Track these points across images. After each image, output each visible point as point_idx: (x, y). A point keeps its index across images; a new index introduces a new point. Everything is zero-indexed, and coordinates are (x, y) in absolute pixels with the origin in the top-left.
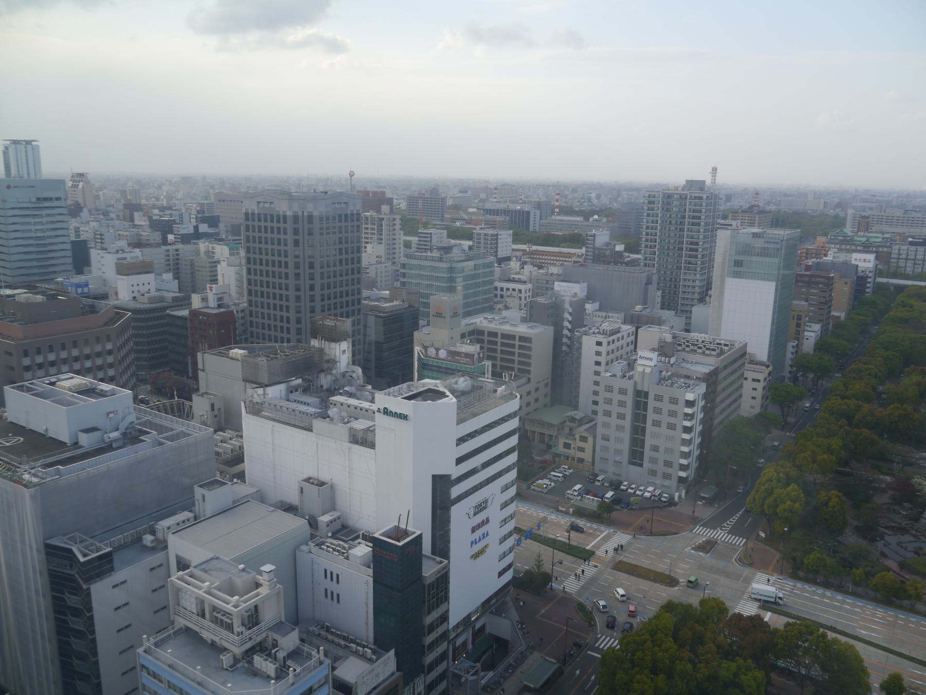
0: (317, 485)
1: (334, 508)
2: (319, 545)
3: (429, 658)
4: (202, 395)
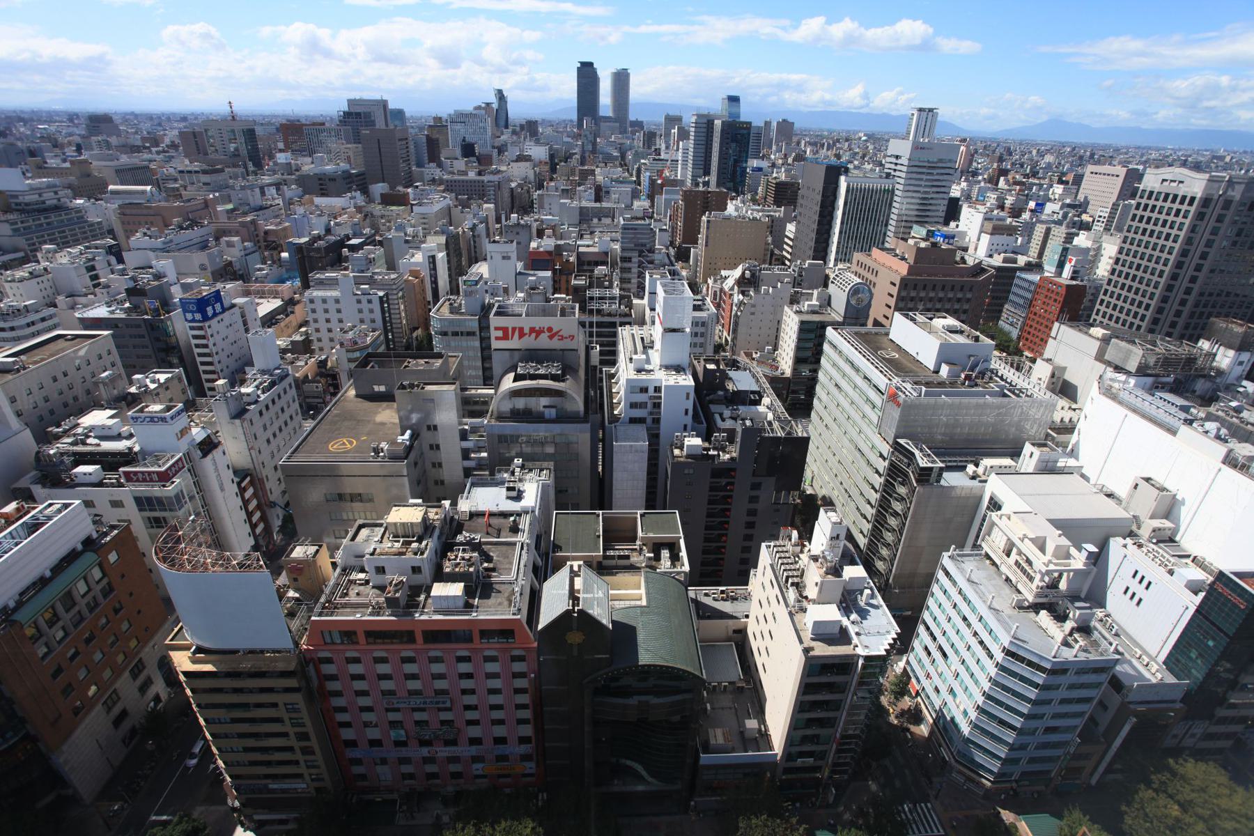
0: (1158, 488)
1: (1167, 516)
2: (1140, 546)
3: (1221, 712)
4: (1048, 360)
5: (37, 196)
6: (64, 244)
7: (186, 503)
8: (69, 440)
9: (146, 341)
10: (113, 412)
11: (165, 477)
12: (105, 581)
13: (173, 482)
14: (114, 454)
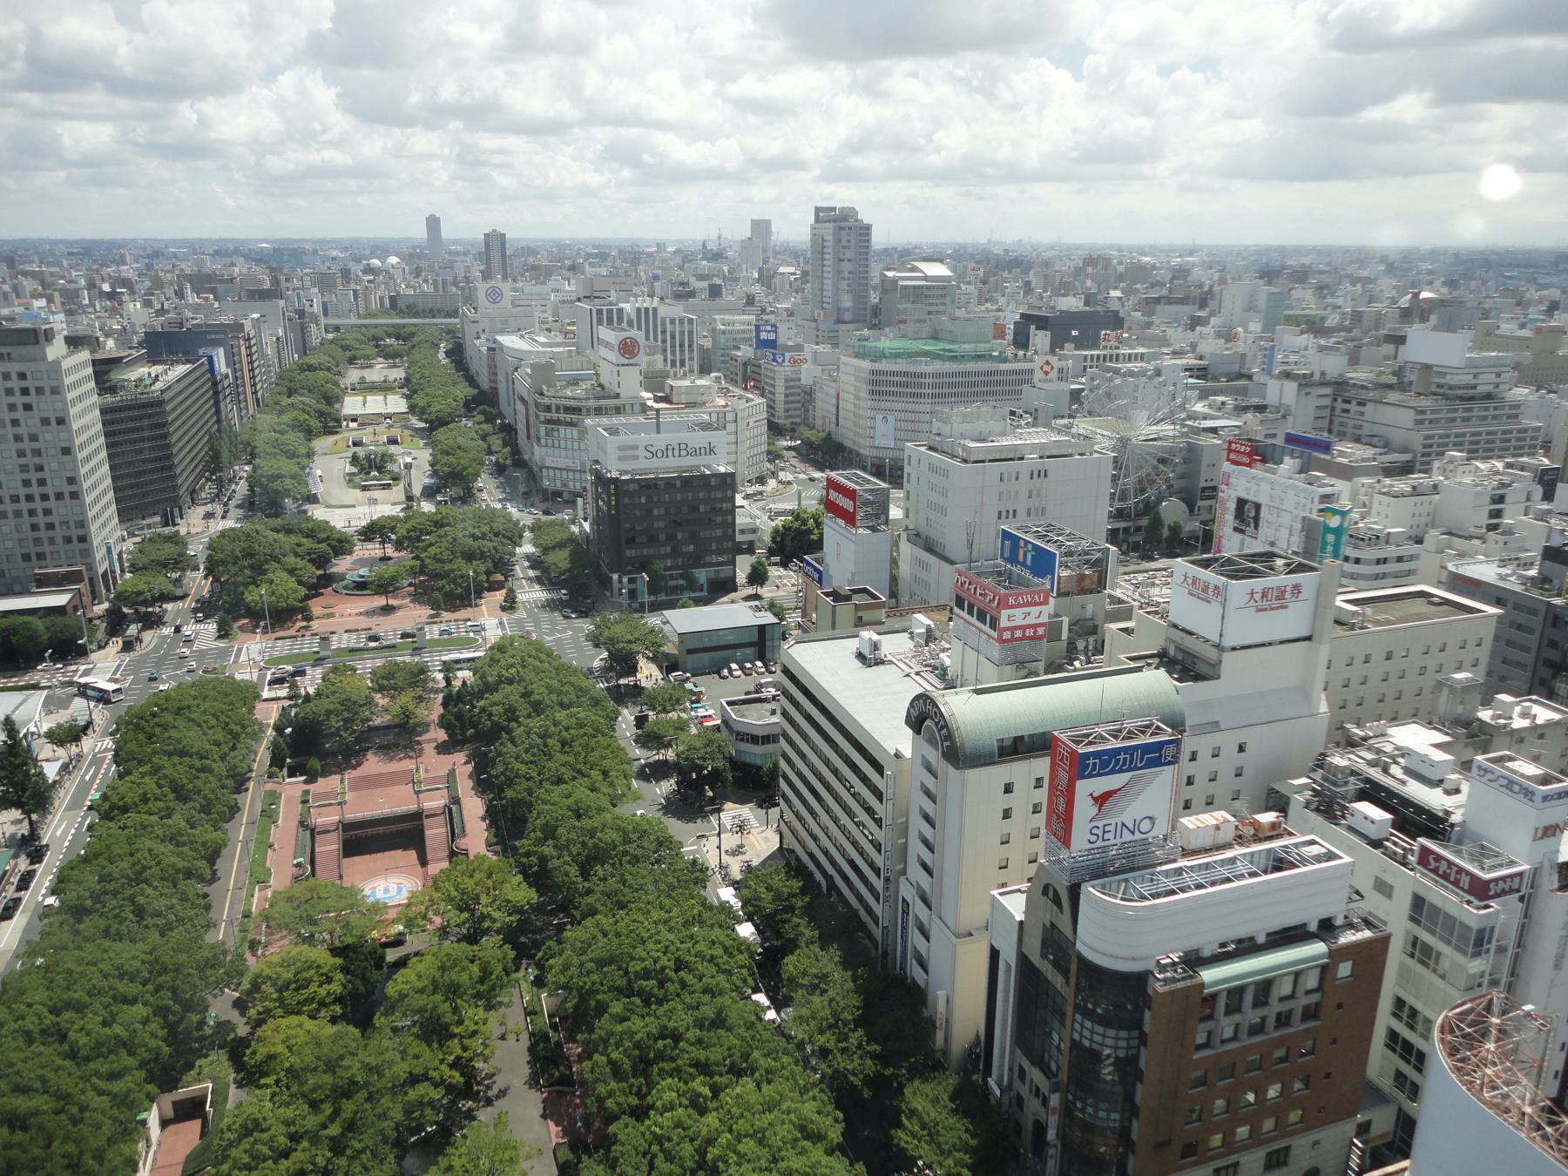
5: (1471, 377)
6: (1478, 449)
7: (1488, 951)
8: (1370, 756)
9: (1533, 640)
10: (1447, 739)
11: (1481, 891)
12: (1315, 998)
13: (1487, 907)
14: (1420, 810)
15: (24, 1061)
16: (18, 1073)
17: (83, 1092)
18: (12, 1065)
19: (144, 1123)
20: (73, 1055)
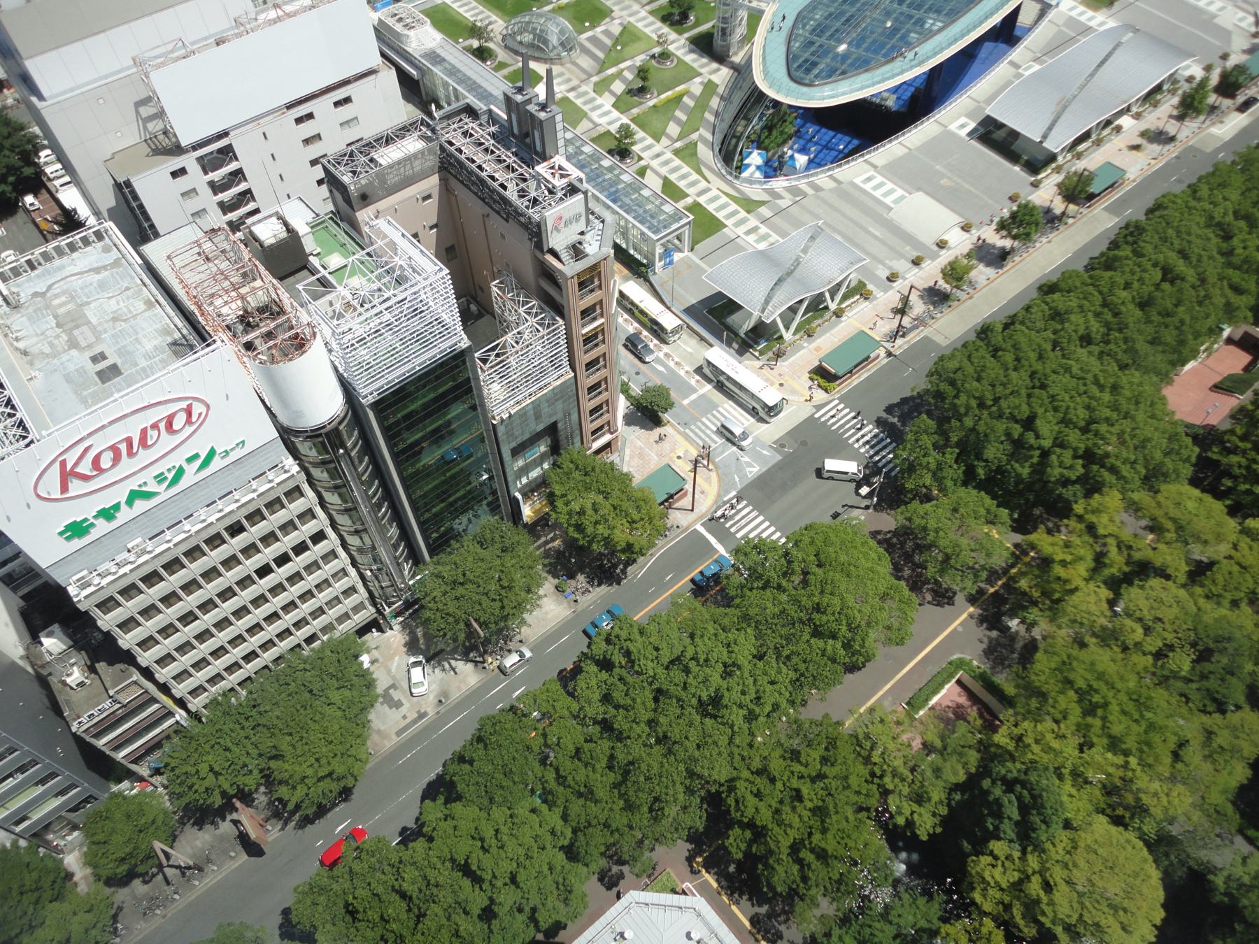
15: (1198, 236)
16: (1189, 242)
17: (1214, 286)
18: (1189, 234)
19: (1222, 330)
20: (1229, 253)
